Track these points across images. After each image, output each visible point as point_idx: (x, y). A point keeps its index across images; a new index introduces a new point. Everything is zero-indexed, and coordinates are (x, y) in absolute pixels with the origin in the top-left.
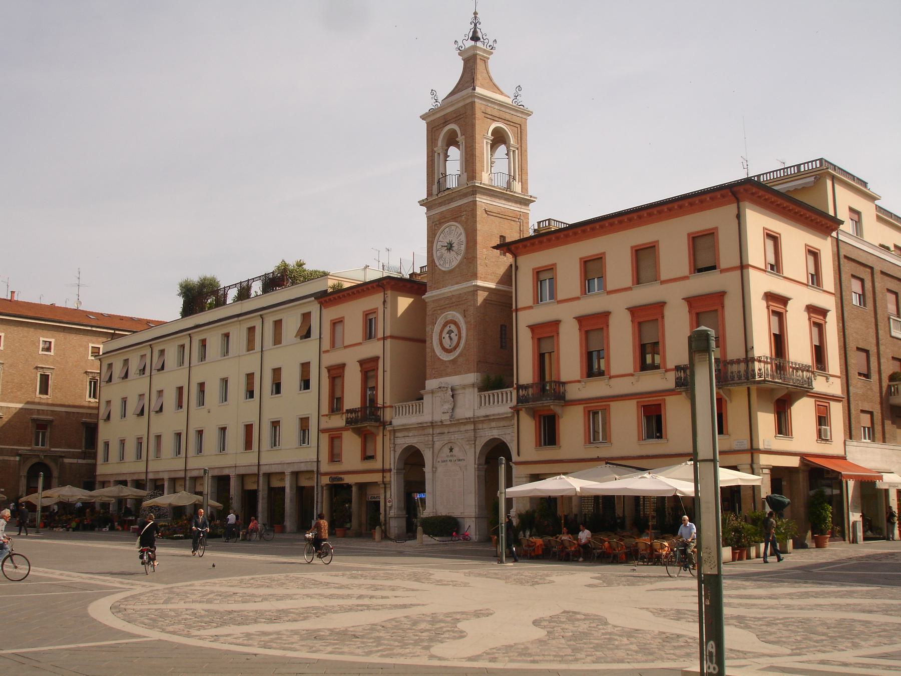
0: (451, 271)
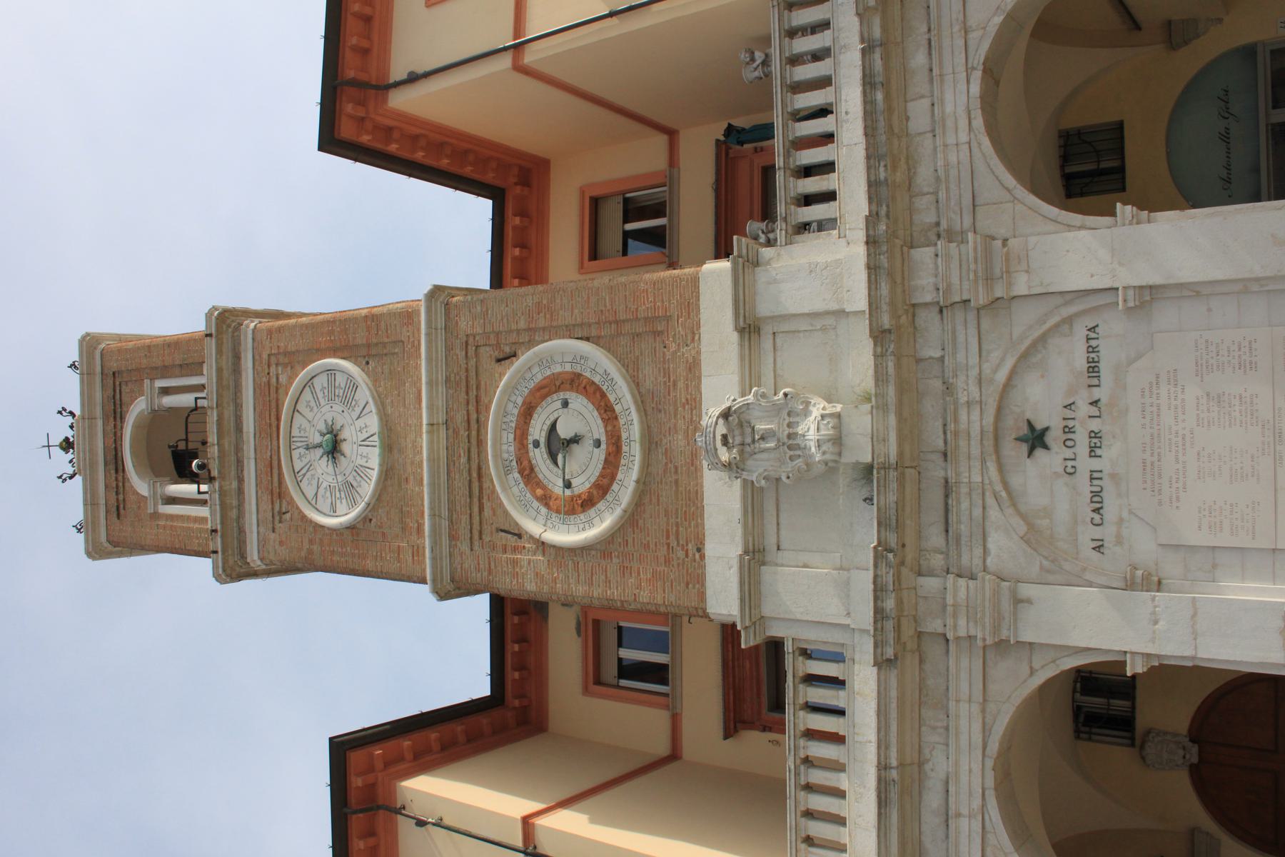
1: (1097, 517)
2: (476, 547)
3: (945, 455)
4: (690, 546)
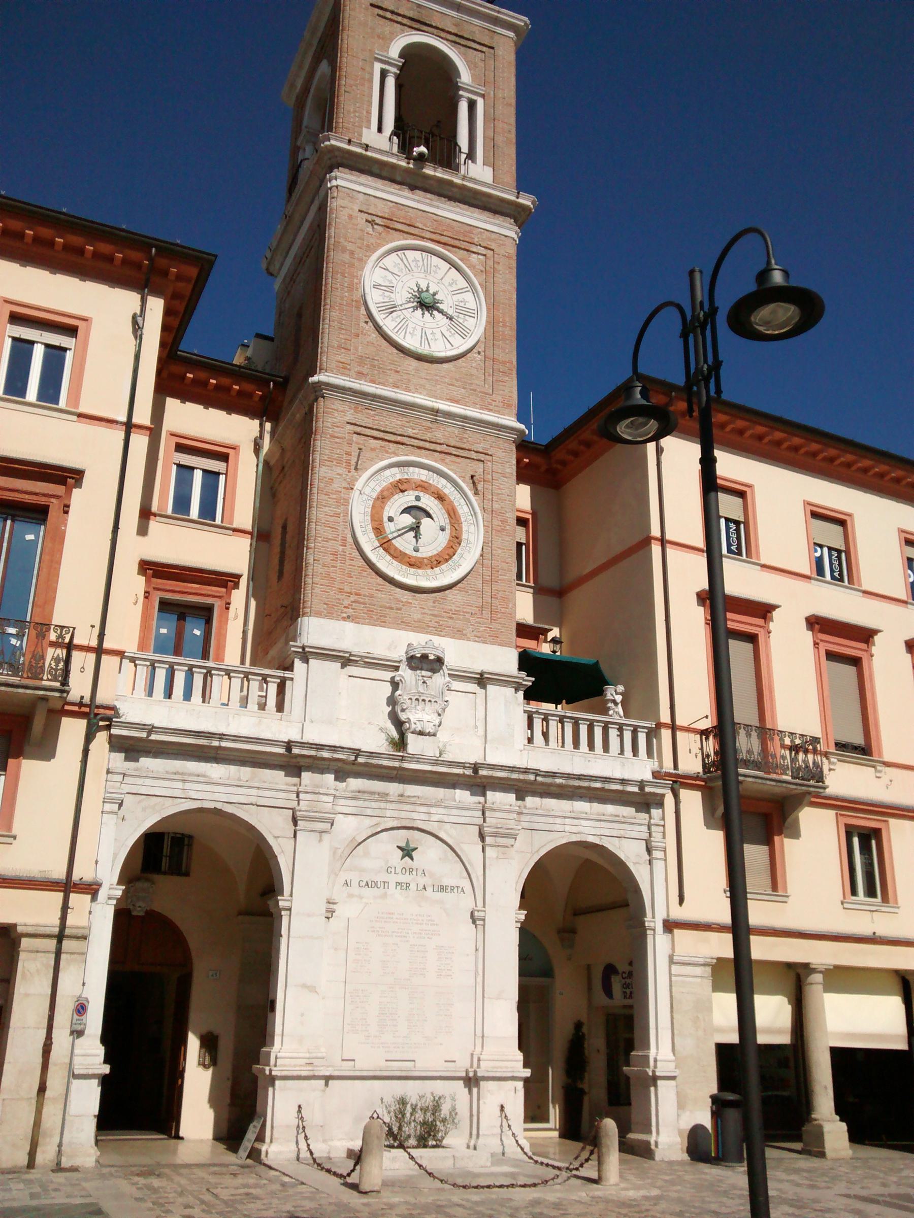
0: (420, 358)
1: (363, 884)
2: (349, 426)
3: (402, 795)
4: (351, 611)
